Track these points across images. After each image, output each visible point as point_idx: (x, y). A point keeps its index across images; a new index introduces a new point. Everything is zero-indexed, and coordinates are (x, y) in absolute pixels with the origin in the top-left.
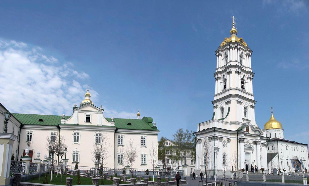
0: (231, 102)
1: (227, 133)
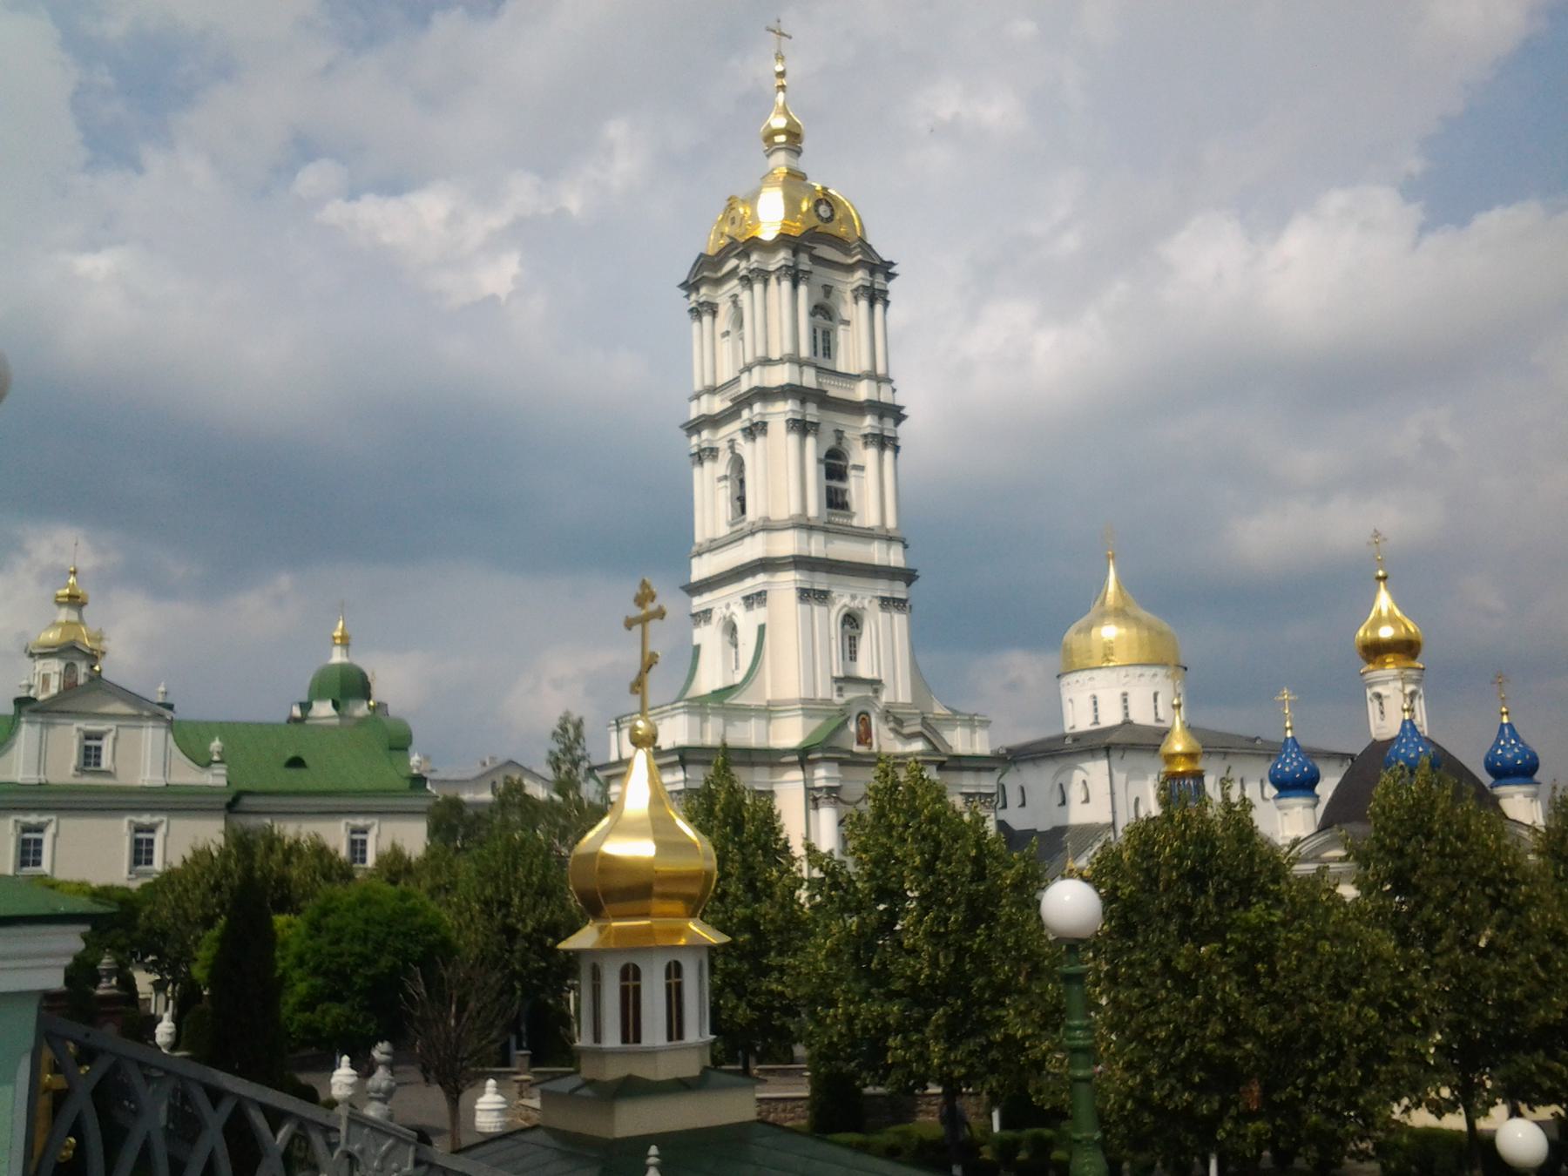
1: (753, 764)
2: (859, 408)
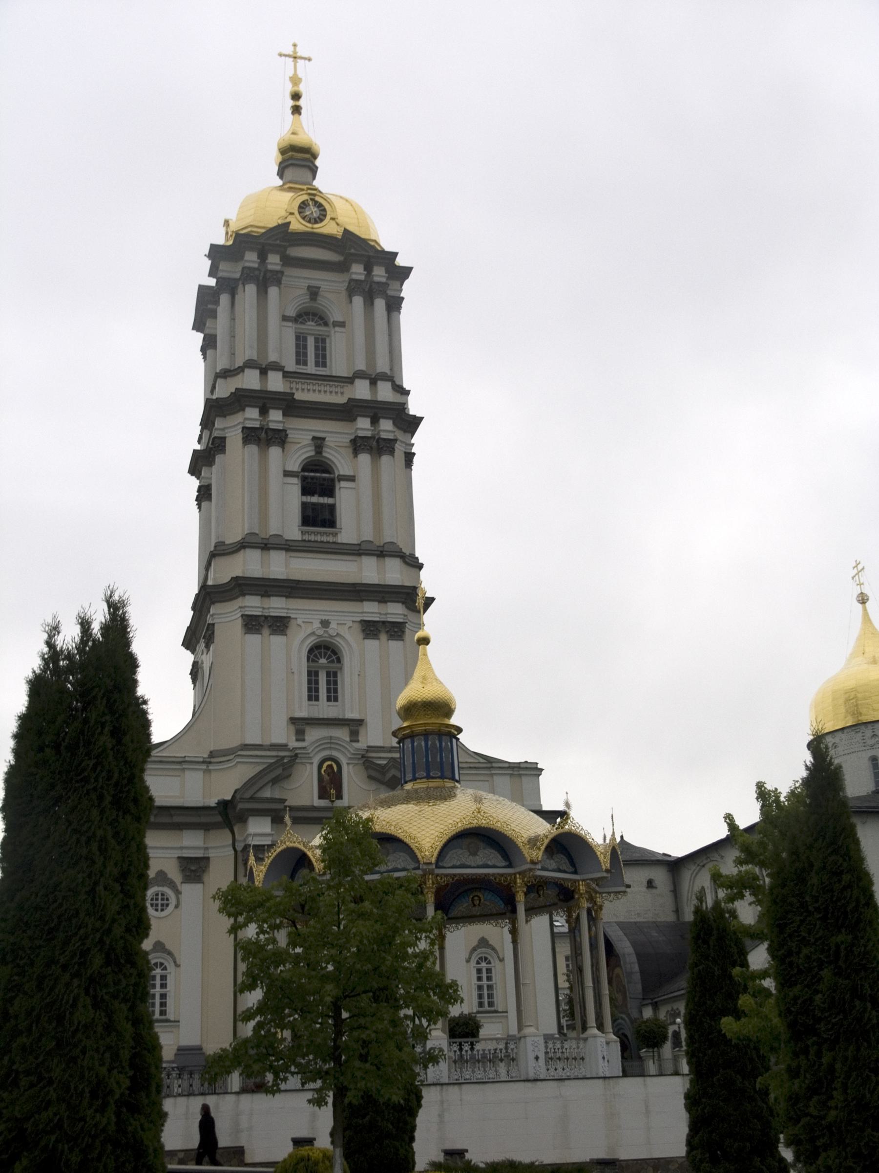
0: (216, 626)
1: (180, 827)
2: (348, 412)
